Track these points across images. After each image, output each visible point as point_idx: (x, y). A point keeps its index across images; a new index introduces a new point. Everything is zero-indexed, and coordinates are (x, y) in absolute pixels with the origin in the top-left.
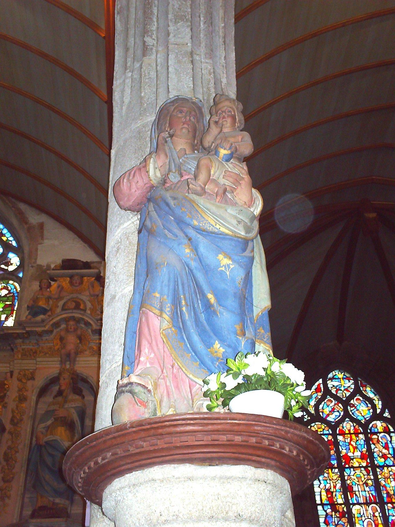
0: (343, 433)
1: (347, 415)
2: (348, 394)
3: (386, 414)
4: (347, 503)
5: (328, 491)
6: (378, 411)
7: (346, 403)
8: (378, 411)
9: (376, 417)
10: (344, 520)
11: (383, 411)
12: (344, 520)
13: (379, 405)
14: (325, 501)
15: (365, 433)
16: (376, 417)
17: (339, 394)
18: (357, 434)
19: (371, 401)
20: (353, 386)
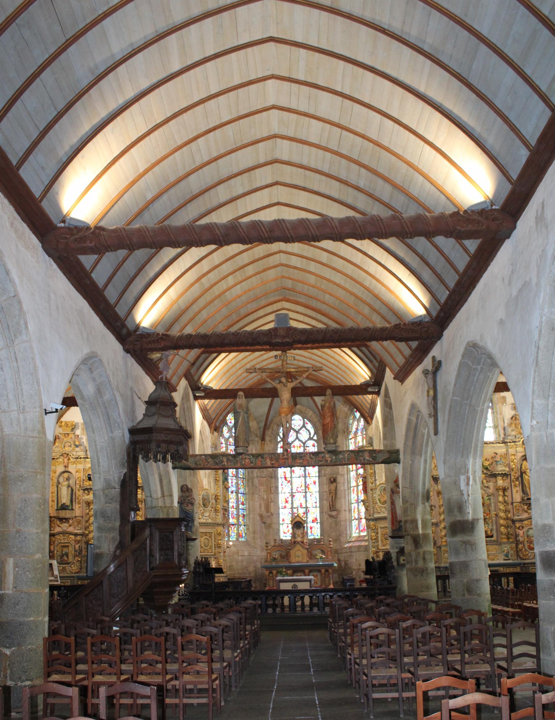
0: (294, 447)
1: (297, 438)
2: (299, 428)
3: (315, 438)
4: (291, 477)
5: (284, 472)
6: (311, 436)
7: (297, 432)
8: (311, 436)
9: (310, 439)
10: (289, 484)
11: (314, 436)
12: (289, 484)
13: (312, 431)
14: (283, 476)
15: (304, 446)
16: (310, 439)
17: (295, 428)
18: (300, 447)
19: (309, 431)
20: (302, 424)
